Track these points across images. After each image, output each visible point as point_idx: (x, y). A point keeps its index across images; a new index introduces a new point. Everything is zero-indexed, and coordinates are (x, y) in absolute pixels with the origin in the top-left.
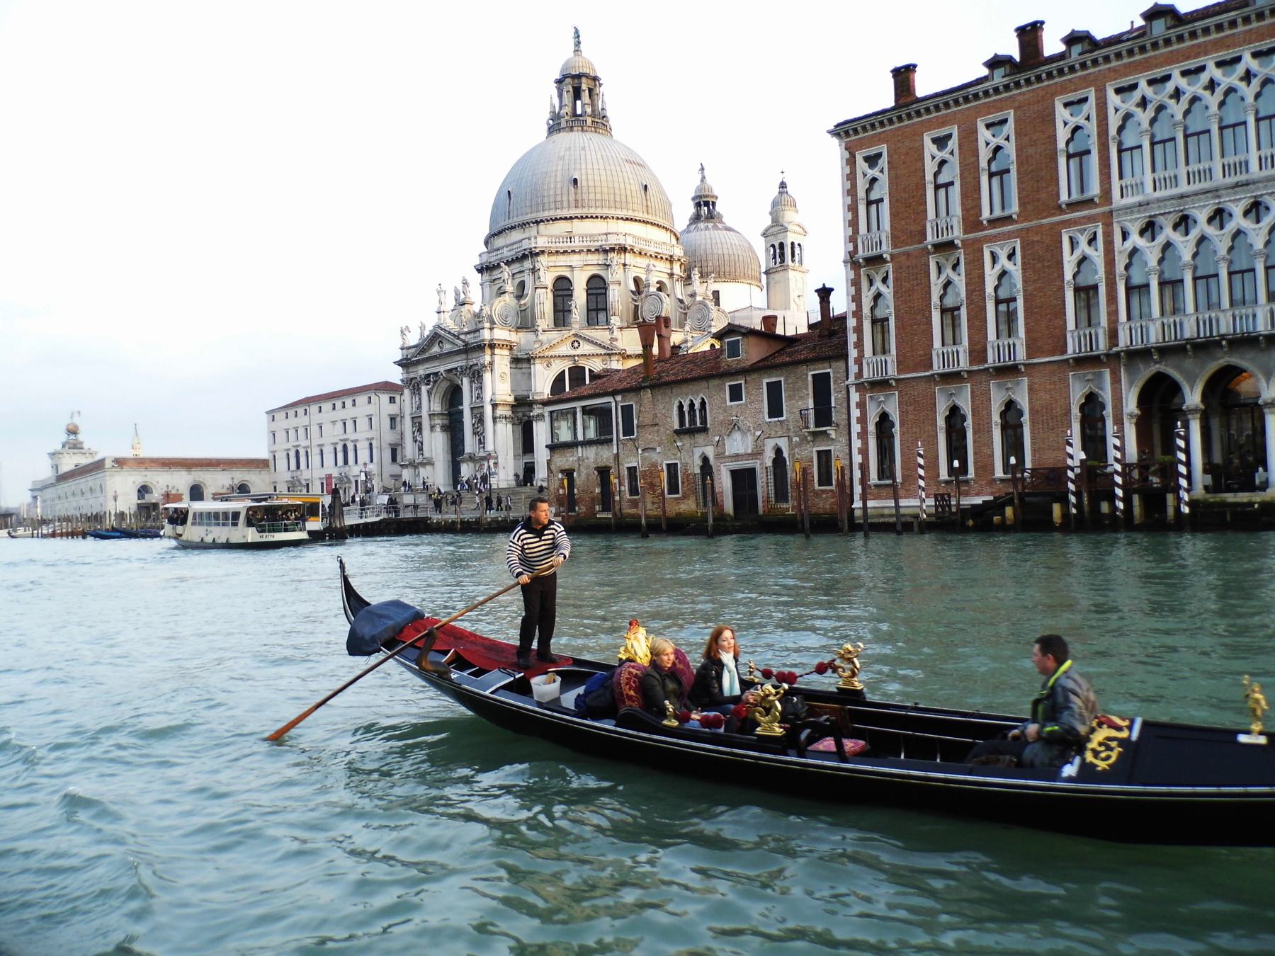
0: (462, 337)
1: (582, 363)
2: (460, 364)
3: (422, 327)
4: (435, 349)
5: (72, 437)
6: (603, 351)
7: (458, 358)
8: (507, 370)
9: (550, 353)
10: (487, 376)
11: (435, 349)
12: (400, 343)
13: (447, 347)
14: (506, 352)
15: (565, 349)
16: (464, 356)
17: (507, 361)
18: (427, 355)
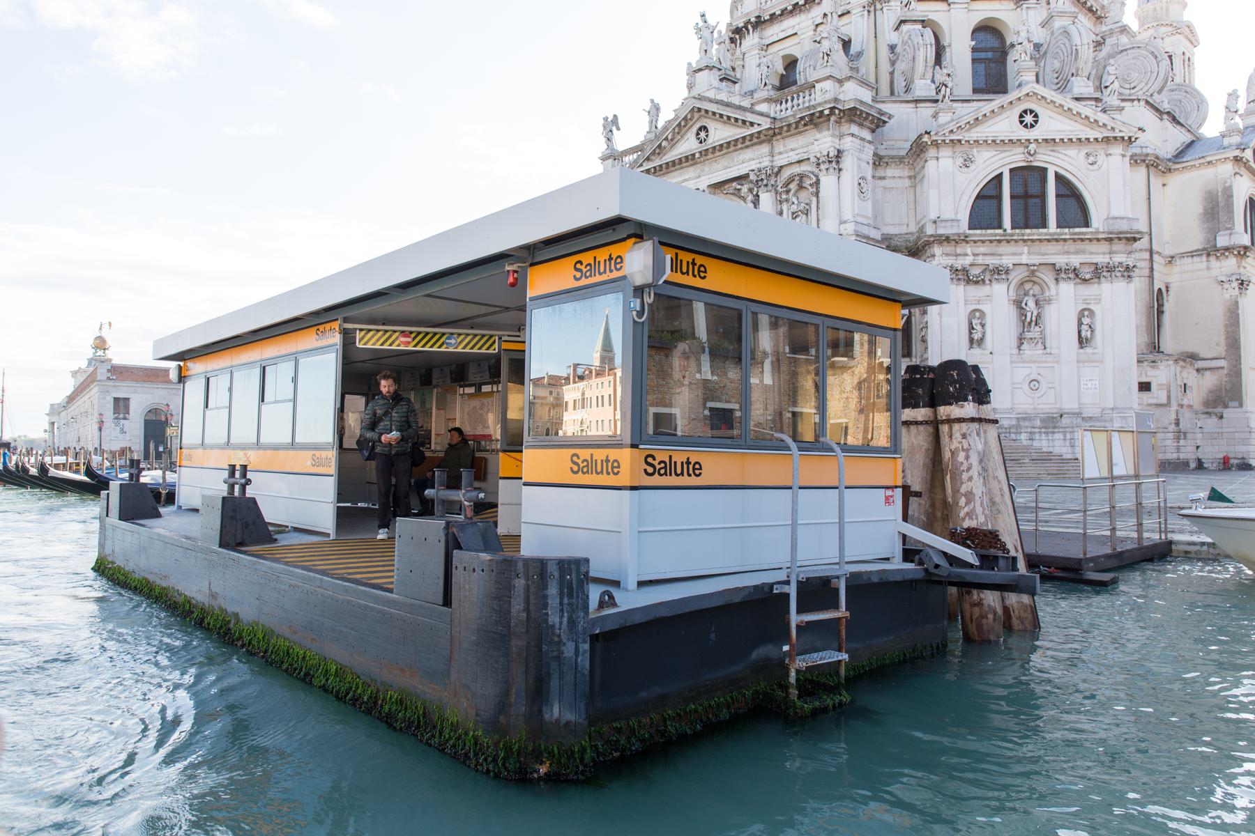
0: (763, 107)
1: (1043, 158)
2: (754, 165)
3: (655, 109)
4: (688, 144)
5: (100, 353)
6: (1092, 134)
7: (748, 154)
8: (869, 171)
9: (974, 134)
10: (828, 182)
11: (688, 144)
12: (602, 147)
13: (719, 133)
14: (866, 134)
15: (1006, 126)
16: (765, 149)
17: (869, 151)
18: (668, 157)
